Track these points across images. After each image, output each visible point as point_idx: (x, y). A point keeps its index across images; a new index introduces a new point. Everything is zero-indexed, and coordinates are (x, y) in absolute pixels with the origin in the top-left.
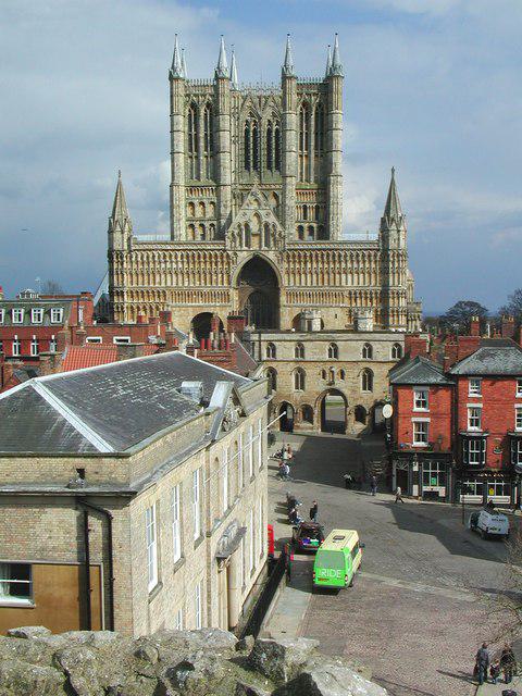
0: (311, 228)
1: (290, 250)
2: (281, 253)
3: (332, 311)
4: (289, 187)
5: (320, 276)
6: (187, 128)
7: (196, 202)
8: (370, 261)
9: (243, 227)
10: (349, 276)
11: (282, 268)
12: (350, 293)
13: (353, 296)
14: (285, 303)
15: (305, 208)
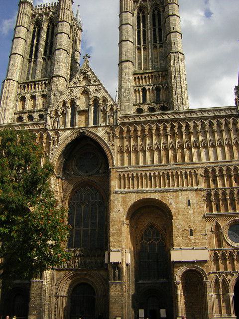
0: (151, 109)
1: (124, 124)
2: (112, 129)
3: (183, 197)
4: (125, 70)
5: (163, 153)
6: (29, 40)
7: (28, 96)
8: (229, 131)
9: (68, 105)
10: (203, 151)
11: (113, 147)
12: (206, 171)
13: (210, 175)
14: (118, 189)
15: (144, 90)
